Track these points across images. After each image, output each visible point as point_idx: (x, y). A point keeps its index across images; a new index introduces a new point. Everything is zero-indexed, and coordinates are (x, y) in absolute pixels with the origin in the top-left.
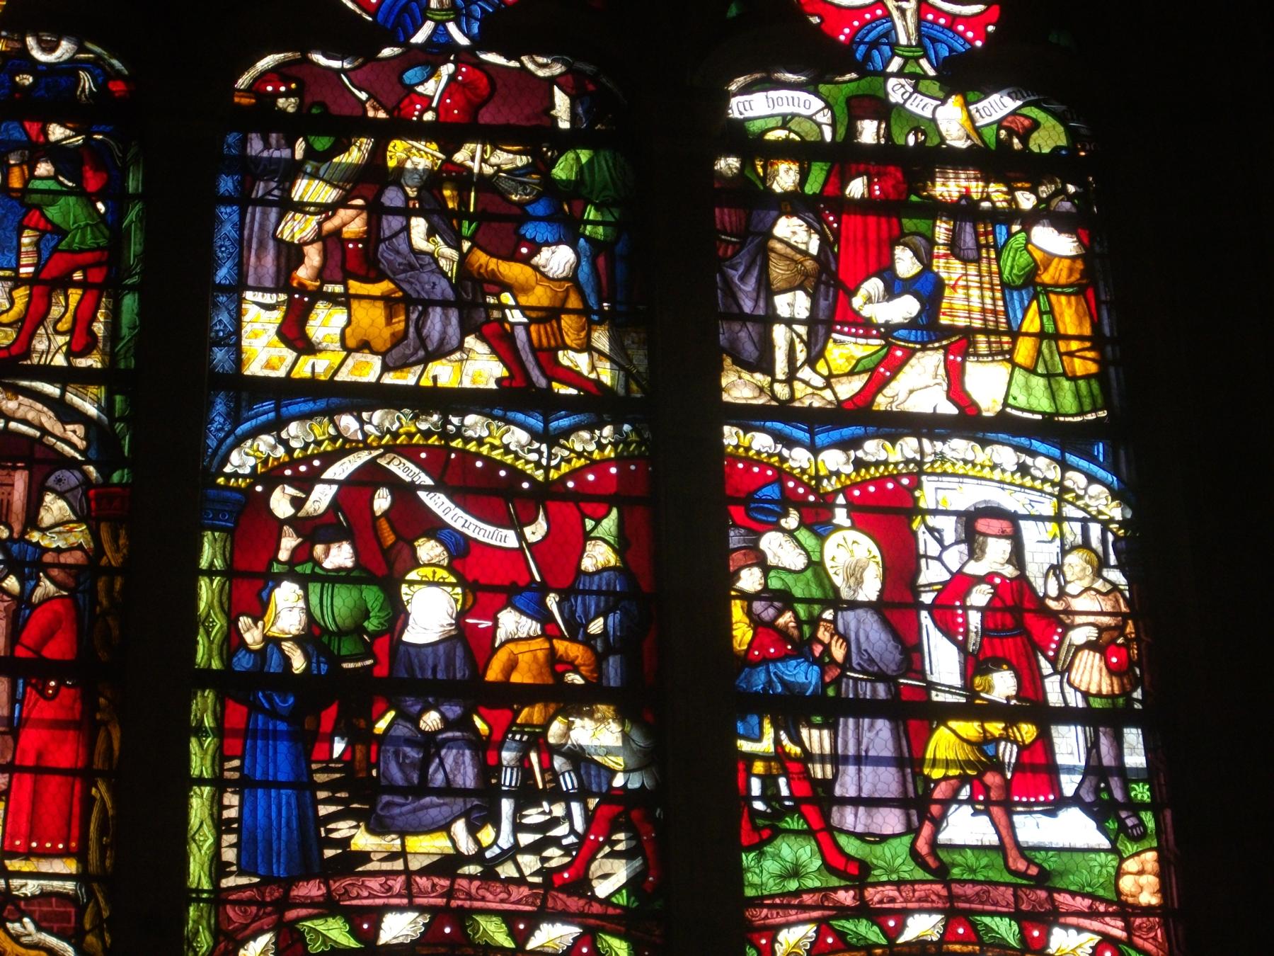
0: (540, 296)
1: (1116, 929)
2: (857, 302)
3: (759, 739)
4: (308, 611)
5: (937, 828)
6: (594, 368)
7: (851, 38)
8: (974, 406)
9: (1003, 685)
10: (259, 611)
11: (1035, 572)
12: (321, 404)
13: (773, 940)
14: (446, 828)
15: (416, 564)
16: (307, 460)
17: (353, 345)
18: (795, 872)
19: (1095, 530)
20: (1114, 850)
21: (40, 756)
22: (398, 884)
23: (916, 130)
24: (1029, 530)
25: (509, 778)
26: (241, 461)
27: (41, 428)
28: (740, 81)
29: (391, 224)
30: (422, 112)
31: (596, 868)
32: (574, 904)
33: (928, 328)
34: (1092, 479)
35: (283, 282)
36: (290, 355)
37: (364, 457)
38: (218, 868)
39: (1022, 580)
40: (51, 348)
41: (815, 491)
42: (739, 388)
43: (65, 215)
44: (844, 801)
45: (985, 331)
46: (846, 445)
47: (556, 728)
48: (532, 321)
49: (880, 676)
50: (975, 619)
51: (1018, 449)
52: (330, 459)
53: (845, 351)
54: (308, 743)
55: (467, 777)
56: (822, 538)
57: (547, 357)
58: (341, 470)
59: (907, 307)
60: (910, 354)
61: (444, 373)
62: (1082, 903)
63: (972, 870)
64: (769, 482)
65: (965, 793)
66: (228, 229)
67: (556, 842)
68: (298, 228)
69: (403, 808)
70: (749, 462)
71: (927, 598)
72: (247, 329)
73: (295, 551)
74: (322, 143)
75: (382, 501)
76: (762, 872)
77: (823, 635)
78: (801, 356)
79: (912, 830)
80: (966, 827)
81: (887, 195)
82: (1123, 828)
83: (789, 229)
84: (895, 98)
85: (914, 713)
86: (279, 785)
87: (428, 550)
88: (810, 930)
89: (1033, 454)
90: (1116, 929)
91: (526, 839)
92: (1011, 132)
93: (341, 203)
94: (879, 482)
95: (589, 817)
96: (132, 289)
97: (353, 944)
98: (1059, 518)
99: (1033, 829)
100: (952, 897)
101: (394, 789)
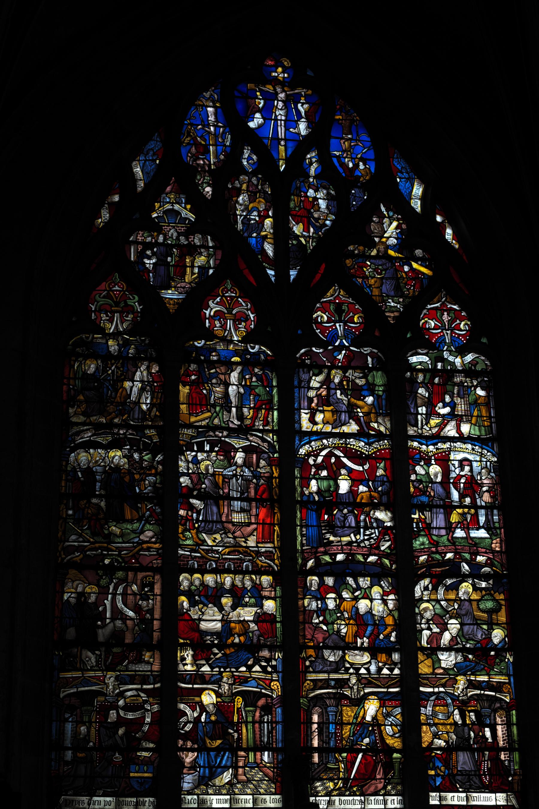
0: (366, 409)
2: (437, 408)
3: (415, 514)
4: (318, 486)
5: (453, 534)
6: (378, 427)
8: (462, 434)
9: (468, 500)
10: (308, 486)
11: (475, 474)
12: (319, 437)
13: (418, 559)
14: (349, 535)
15: (341, 475)
16: (316, 450)
17: (325, 422)
18: (423, 544)
19: (488, 463)
20: (491, 538)
21: (263, 520)
22: (340, 548)
23: (450, 365)
24: (475, 464)
26: (302, 451)
27: (258, 444)
28: (410, 353)
29: (333, 392)
31: (381, 544)
32: (377, 552)
33: (452, 415)
34: (488, 451)
35: (309, 408)
36: (312, 425)
37: (329, 450)
38: (302, 545)
39: (472, 476)
40: (259, 425)
41: (427, 455)
42: (411, 431)
43: (260, 391)
44: (433, 528)
45: (465, 415)
46: (434, 444)
47: (372, 512)
48: (365, 415)
49: (441, 499)
50: (462, 485)
51: (472, 444)
52: (321, 450)
53: (434, 421)
54: (319, 517)
55: (353, 524)
56: (429, 467)
57: (368, 424)
58: (324, 453)
59: (447, 410)
60: (448, 421)
61: (346, 429)
62: (484, 550)
63: (460, 543)
64: (417, 454)
65: (459, 526)
66: (296, 394)
67: (372, 538)
68: (312, 393)
69: (340, 531)
70: (413, 449)
71: (452, 481)
72: (302, 419)
73: (315, 472)
74: (316, 371)
75: (333, 460)
76: (417, 544)
77: (429, 490)
78: (424, 423)
79: (448, 534)
80: (459, 533)
81: (443, 381)
82: (493, 533)
83: (421, 391)
84: (446, 357)
85: (449, 508)
86: (314, 526)
87: (343, 471)
88: (426, 557)
89: (475, 446)
90: (491, 556)
91: (366, 537)
92: (472, 365)
93: (321, 387)
94: (441, 453)
95: (379, 532)
96: (276, 409)
97: (330, 561)
98: (481, 461)
99: (474, 534)
100: (456, 549)
101: (338, 527)
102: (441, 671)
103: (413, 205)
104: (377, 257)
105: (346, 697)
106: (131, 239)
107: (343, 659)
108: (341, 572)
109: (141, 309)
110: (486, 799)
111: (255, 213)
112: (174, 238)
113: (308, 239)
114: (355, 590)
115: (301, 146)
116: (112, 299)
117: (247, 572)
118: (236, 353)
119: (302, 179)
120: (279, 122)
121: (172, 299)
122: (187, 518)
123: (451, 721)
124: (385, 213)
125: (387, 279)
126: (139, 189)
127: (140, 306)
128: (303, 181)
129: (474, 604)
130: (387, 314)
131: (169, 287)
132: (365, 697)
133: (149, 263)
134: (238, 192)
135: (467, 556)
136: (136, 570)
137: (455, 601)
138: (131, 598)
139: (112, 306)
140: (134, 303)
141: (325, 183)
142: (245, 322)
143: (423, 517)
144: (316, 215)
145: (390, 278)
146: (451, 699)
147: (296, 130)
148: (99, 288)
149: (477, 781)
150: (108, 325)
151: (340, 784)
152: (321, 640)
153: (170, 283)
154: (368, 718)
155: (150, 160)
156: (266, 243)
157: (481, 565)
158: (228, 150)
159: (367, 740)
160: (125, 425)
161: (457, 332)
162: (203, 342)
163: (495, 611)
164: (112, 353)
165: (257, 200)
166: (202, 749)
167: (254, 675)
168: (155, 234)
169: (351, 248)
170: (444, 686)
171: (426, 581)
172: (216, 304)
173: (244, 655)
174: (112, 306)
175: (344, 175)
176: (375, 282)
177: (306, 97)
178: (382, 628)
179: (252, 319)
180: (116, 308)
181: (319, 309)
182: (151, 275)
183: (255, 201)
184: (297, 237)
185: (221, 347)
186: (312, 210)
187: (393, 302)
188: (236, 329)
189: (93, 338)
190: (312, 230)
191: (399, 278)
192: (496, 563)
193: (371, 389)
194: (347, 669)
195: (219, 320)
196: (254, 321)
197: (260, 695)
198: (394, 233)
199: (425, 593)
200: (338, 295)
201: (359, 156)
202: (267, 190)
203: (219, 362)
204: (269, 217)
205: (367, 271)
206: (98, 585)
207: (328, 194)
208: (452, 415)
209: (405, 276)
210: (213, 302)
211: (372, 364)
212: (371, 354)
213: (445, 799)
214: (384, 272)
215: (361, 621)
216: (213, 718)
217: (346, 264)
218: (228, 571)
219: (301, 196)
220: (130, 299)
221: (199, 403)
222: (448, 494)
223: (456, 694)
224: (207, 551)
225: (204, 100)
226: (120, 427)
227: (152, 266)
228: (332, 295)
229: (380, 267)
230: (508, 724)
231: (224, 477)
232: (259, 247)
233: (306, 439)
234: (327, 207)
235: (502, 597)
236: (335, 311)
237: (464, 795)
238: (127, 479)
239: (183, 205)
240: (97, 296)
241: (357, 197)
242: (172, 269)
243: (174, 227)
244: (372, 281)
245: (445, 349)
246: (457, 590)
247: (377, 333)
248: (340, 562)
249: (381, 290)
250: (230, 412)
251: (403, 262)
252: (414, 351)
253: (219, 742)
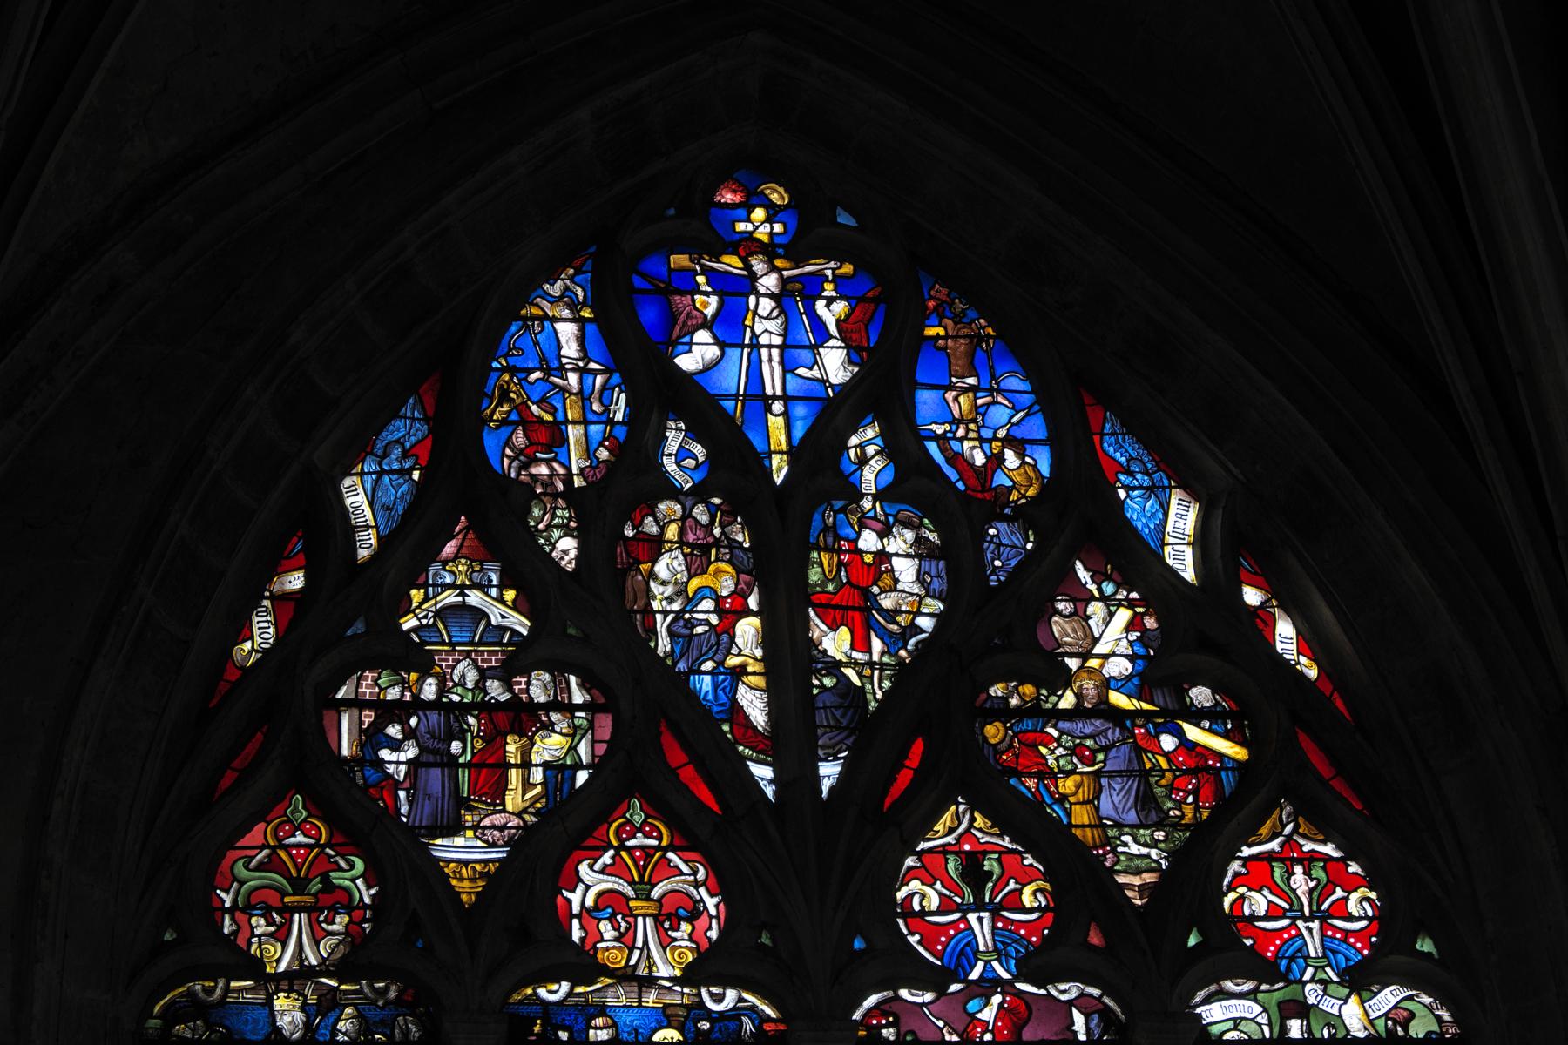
7: (1276, 953)
30: (983, 1034)
103: (1170, 562)
104: (1077, 713)
106: (340, 695)
109: (373, 897)
111: (707, 605)
112: (470, 685)
113: (867, 672)
115: (832, 414)
116: (282, 870)
118: (666, 1016)
119: (839, 504)
120: (764, 352)
121: (466, 863)
124: (1093, 587)
125: (1111, 775)
126: (363, 554)
127: (369, 887)
128: (843, 510)
130: (1121, 879)
131: (456, 829)
133: (397, 761)
134: (655, 546)
139: (284, 894)
140: (353, 880)
141: (908, 512)
142: (690, 920)
144: (887, 602)
145: (1120, 773)
147: (815, 373)
148: (247, 840)
150: (273, 950)
153: (459, 816)
155: (393, 472)
156: (742, 689)
158: (621, 433)
161: (1335, 922)
162: (565, 986)
164: (286, 1033)
165: (712, 568)
168: (414, 676)
169: (997, 690)
172: (601, 872)
174: (284, 894)
175: (960, 485)
176: (1078, 786)
177: (838, 280)
179: (713, 912)
180: (296, 899)
181: (912, 874)
182: (402, 794)
183: (705, 572)
184: (834, 667)
185: (618, 997)
186: (875, 589)
187: (1136, 841)
188: (666, 943)
189: (227, 990)
190: (877, 645)
191: (1148, 773)
195: (611, 919)
196: (718, 917)
198: (1124, 643)
200: (968, 830)
201: (1002, 433)
202: (740, 538)
204: (748, 613)
205: (1052, 756)
207: (919, 540)
209: (1165, 765)
210: (591, 867)
211: (1088, 1031)
212: (1082, 1001)
214: (1100, 757)
217: (985, 739)
219: (840, 551)
220: (341, 869)
225: (545, 305)
227: (403, 768)
228: (951, 831)
229: (1089, 742)
232: (723, 698)
234: (920, 578)
236: (962, 875)
239: (494, 592)
240: (240, 863)
241: (1006, 547)
242: (464, 776)
243: (468, 654)
244: (1067, 785)
245: (1307, 977)
247: (1095, 938)
249: (1097, 809)
251: (1156, 725)
252: (1213, 988)
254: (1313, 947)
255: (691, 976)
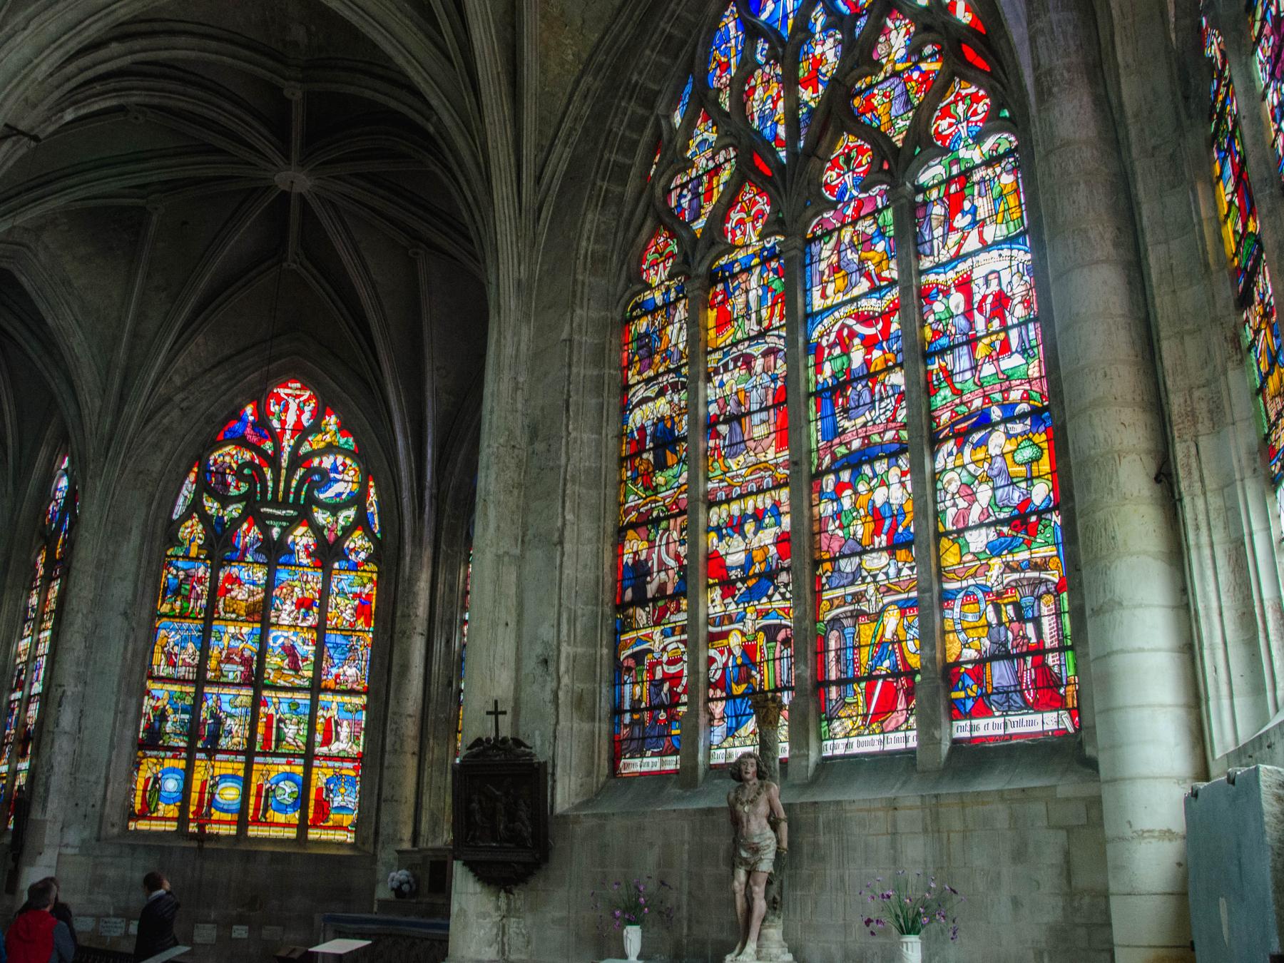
0: (877, 259)
1: (1027, 387)
9: (996, 323)
25: (877, 397)
32: (893, 425)
38: (818, 442)
40: (776, 322)
46: (952, 269)
50: (988, 307)
53: (954, 237)
54: (835, 404)
59: (969, 218)
61: (856, 292)
75: (845, 332)
76: (938, 401)
79: (973, 376)
80: (988, 370)
90: (1027, 387)
102: (970, 557)
104: (886, 79)
105: (863, 613)
107: (859, 566)
108: (855, 462)
110: (1031, 723)
114: (871, 479)
117: (769, 489)
122: (717, 448)
123: (983, 621)
129: (1009, 457)
132: (883, 610)
133: (685, 203)
134: (753, 89)
135: (998, 397)
136: (675, 516)
137: (984, 460)
138: (672, 546)
143: (943, 364)
144: (824, 70)
146: (983, 592)
149: (1018, 700)
151: (859, 722)
152: (837, 549)
154: (888, 636)
157: (1014, 405)
159: (887, 663)
160: (668, 371)
163: (1036, 460)
166: (730, 697)
167: (775, 605)
169: (858, 85)
170: (974, 576)
171: (950, 445)
173: (765, 582)
178: (900, 518)
184: (806, 104)
192: (1034, 394)
193: (881, 233)
194: (864, 578)
197: (779, 628)
199: (952, 458)
203: (742, 271)
206: (648, 540)
208: (974, 223)
213: (977, 728)
215: (877, 515)
216: (739, 661)
218: (751, 493)
221: (725, 321)
222: (972, 325)
223: (989, 584)
224: (732, 478)
226: (663, 374)
230: (1058, 614)
231: (745, 391)
233: (819, 318)
235: (1044, 437)
237: (1001, 720)
238: (669, 425)
246: (986, 445)
248: (856, 451)
250: (749, 320)
253: (744, 686)
254: (964, 134)
255: (762, 237)
